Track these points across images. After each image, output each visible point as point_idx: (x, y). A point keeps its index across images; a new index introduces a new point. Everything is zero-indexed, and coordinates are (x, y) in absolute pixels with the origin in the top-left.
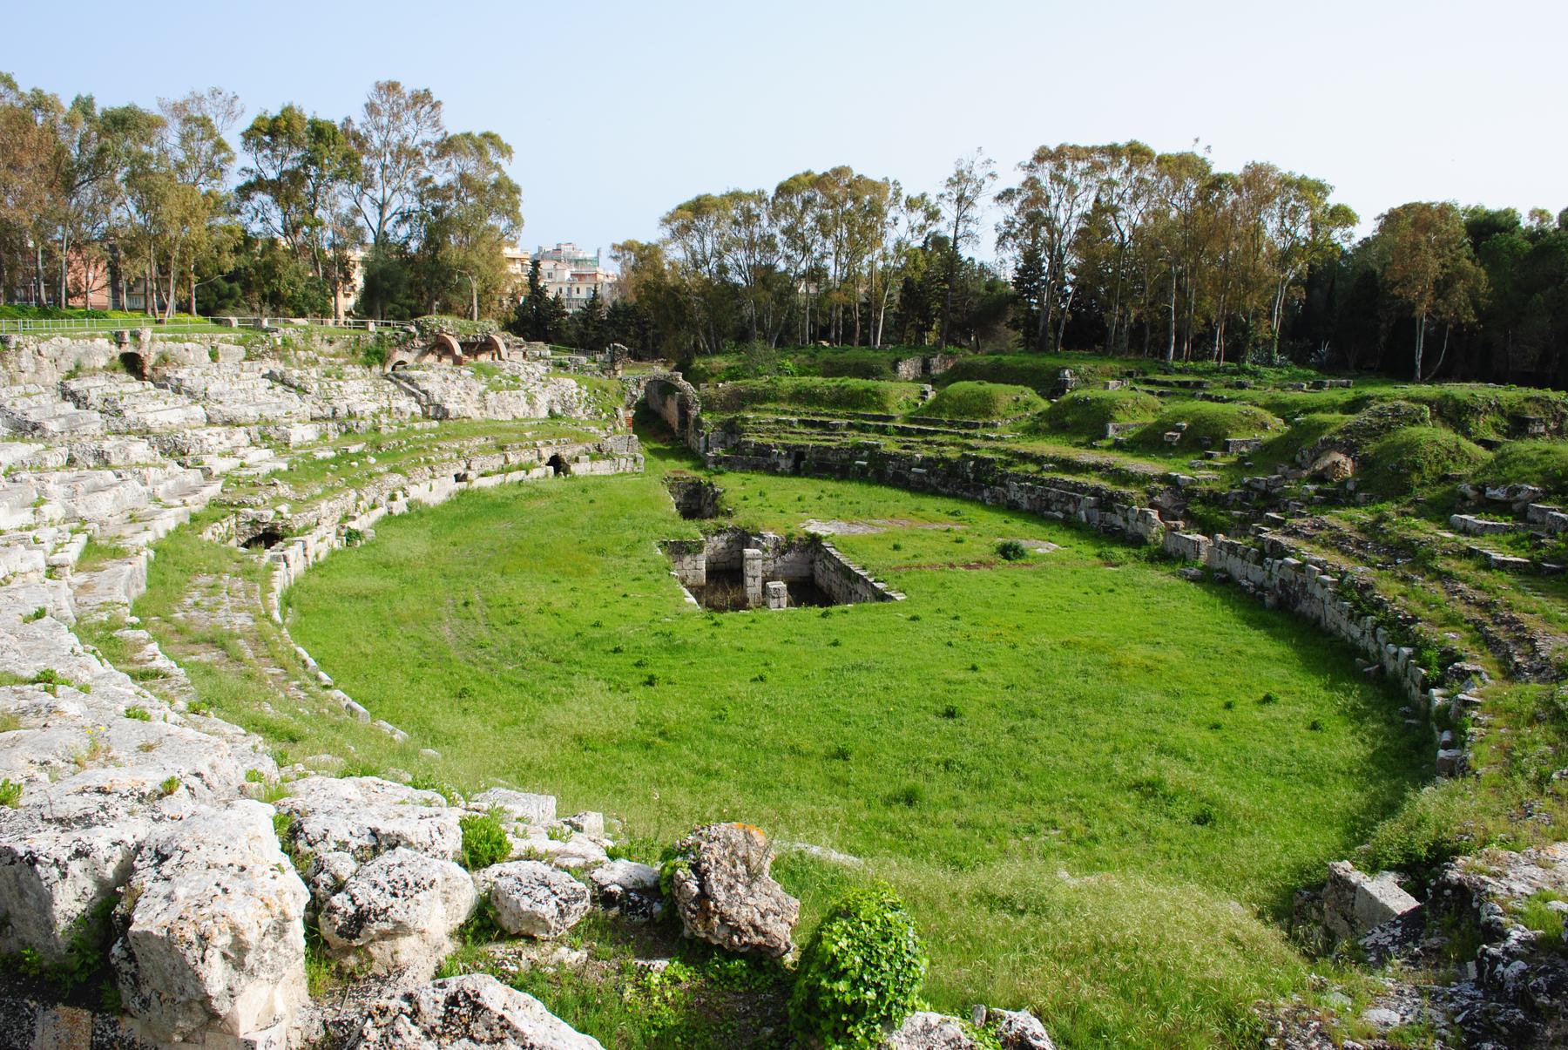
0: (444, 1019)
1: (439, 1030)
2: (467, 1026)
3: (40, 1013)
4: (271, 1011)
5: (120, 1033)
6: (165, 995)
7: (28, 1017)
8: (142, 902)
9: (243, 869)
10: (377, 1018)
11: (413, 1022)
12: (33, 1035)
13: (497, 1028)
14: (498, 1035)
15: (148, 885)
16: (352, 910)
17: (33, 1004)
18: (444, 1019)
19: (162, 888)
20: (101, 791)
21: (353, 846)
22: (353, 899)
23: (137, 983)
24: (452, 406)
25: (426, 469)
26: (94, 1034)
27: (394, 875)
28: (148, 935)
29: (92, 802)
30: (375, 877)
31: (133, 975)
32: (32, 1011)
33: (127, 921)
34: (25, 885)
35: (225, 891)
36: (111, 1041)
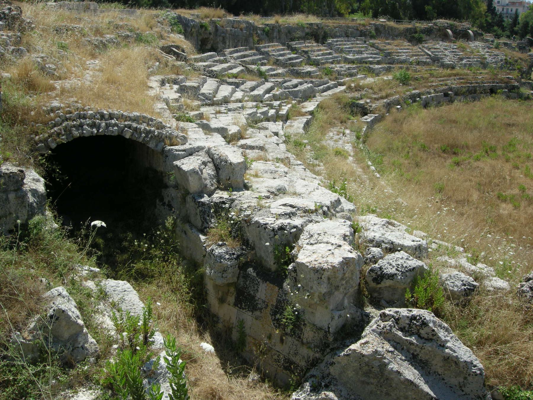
0: (410, 325)
1: (406, 329)
2: (418, 330)
3: (261, 284)
4: (342, 303)
5: (287, 298)
6: (305, 288)
7: (257, 284)
8: (302, 251)
9: (340, 246)
10: (383, 318)
11: (397, 323)
12: (258, 291)
13: (430, 334)
14: (431, 337)
15: (305, 245)
16: (379, 273)
17: (259, 280)
18: (410, 325)
19: (309, 247)
20: (291, 206)
21: (384, 246)
22: (381, 268)
23: (296, 281)
24: (447, 61)
25: (432, 91)
26: (278, 296)
27: (399, 263)
28: (303, 264)
29: (289, 210)
30: (391, 261)
31: (295, 278)
32: (259, 282)
33: (296, 256)
34: (262, 237)
35: (333, 253)
36: (284, 300)
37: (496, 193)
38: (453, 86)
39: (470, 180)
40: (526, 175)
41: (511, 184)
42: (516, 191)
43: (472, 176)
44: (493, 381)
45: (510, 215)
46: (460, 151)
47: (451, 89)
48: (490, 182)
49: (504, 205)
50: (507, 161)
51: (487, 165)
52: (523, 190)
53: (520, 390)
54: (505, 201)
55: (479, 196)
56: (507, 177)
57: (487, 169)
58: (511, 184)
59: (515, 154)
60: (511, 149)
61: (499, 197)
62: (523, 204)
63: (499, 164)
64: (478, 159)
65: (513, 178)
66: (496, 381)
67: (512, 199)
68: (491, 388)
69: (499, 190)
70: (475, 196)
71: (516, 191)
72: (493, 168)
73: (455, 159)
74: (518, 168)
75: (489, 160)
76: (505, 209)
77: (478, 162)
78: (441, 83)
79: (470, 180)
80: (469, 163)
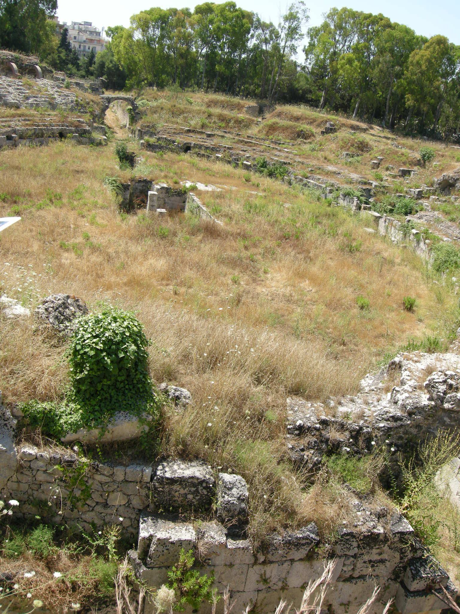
37: (59, 242)
38: (18, 128)
39: (31, 231)
40: (92, 224)
41: (75, 232)
42: (80, 240)
43: (34, 226)
44: (11, 399)
45: (71, 264)
46: (21, 199)
47: (15, 132)
48: (53, 231)
49: (66, 255)
50: (73, 209)
51: (49, 213)
52: (87, 238)
53: (37, 403)
54: (67, 250)
55: (39, 246)
56: (72, 226)
57: (50, 218)
58: (75, 232)
59: (81, 202)
60: (78, 197)
61: (61, 247)
62: (87, 252)
63: (63, 213)
64: (40, 208)
65: (77, 226)
66: (15, 398)
67: (76, 248)
68: (10, 404)
69: (63, 239)
70: (35, 246)
71: (80, 240)
72: (56, 216)
73: (16, 207)
74: (83, 217)
75: (52, 208)
76: (67, 258)
77: (40, 211)
78: (4, 124)
79: (31, 231)
80: (31, 212)
